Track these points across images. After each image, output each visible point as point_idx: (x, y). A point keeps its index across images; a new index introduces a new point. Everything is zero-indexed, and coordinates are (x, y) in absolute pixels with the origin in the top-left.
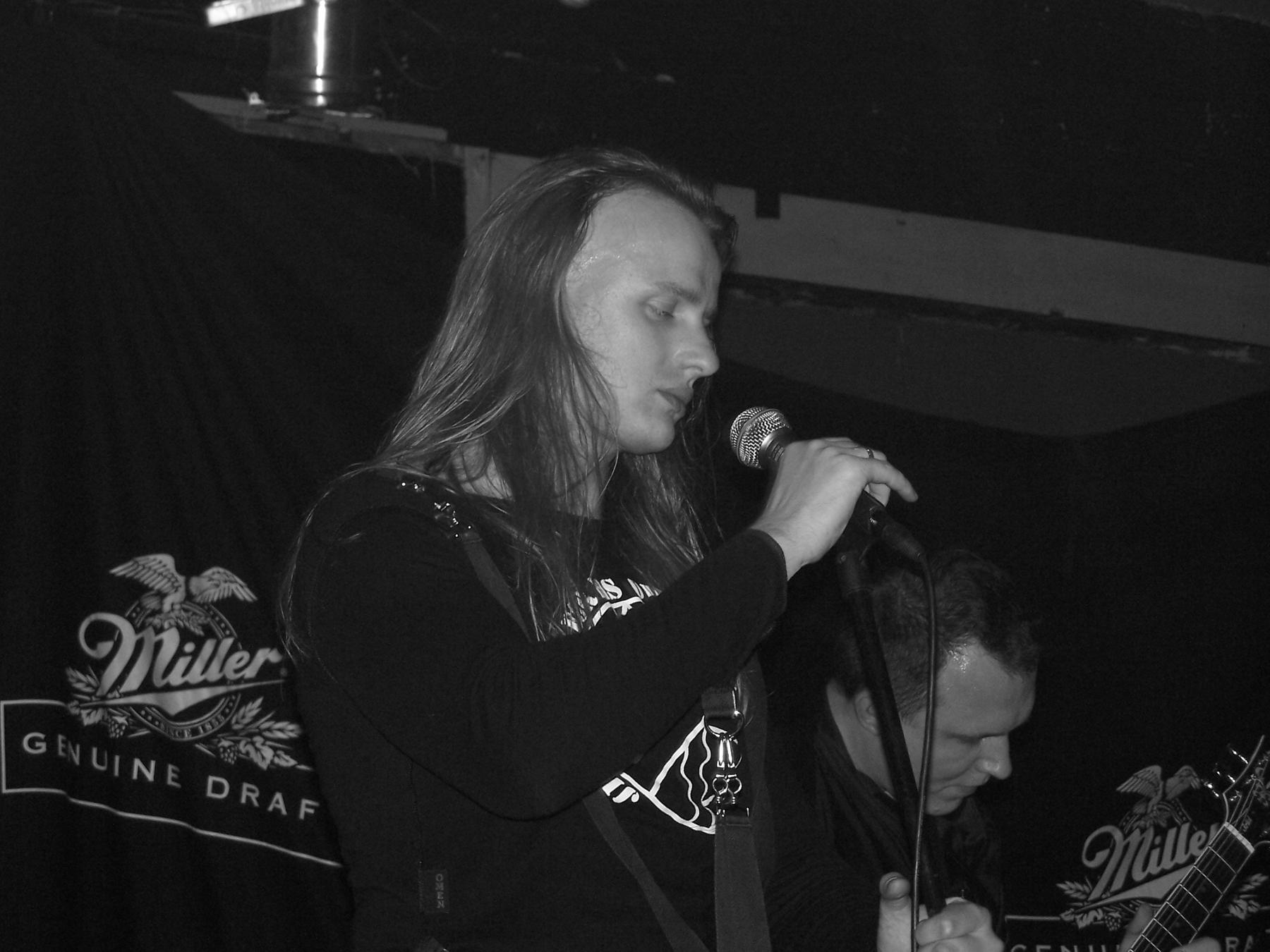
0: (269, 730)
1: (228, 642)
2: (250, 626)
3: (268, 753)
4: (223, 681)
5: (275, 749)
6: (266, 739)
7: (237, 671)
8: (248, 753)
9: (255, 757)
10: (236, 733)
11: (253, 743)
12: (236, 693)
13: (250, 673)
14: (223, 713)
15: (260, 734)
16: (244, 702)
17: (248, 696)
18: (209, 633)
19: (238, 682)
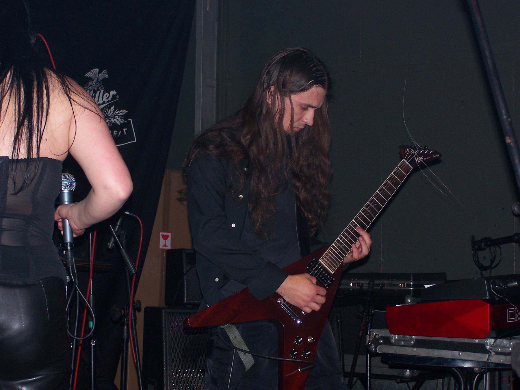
0: (118, 113)
1: (102, 91)
2: (107, 86)
3: (120, 119)
4: (104, 103)
5: (121, 118)
6: (119, 116)
7: (107, 99)
8: (115, 121)
9: (117, 121)
10: (110, 117)
11: (116, 118)
12: (107, 105)
13: (110, 99)
14: (105, 113)
15: (116, 115)
16: (110, 108)
17: (110, 106)
18: (98, 90)
19: (107, 102)
